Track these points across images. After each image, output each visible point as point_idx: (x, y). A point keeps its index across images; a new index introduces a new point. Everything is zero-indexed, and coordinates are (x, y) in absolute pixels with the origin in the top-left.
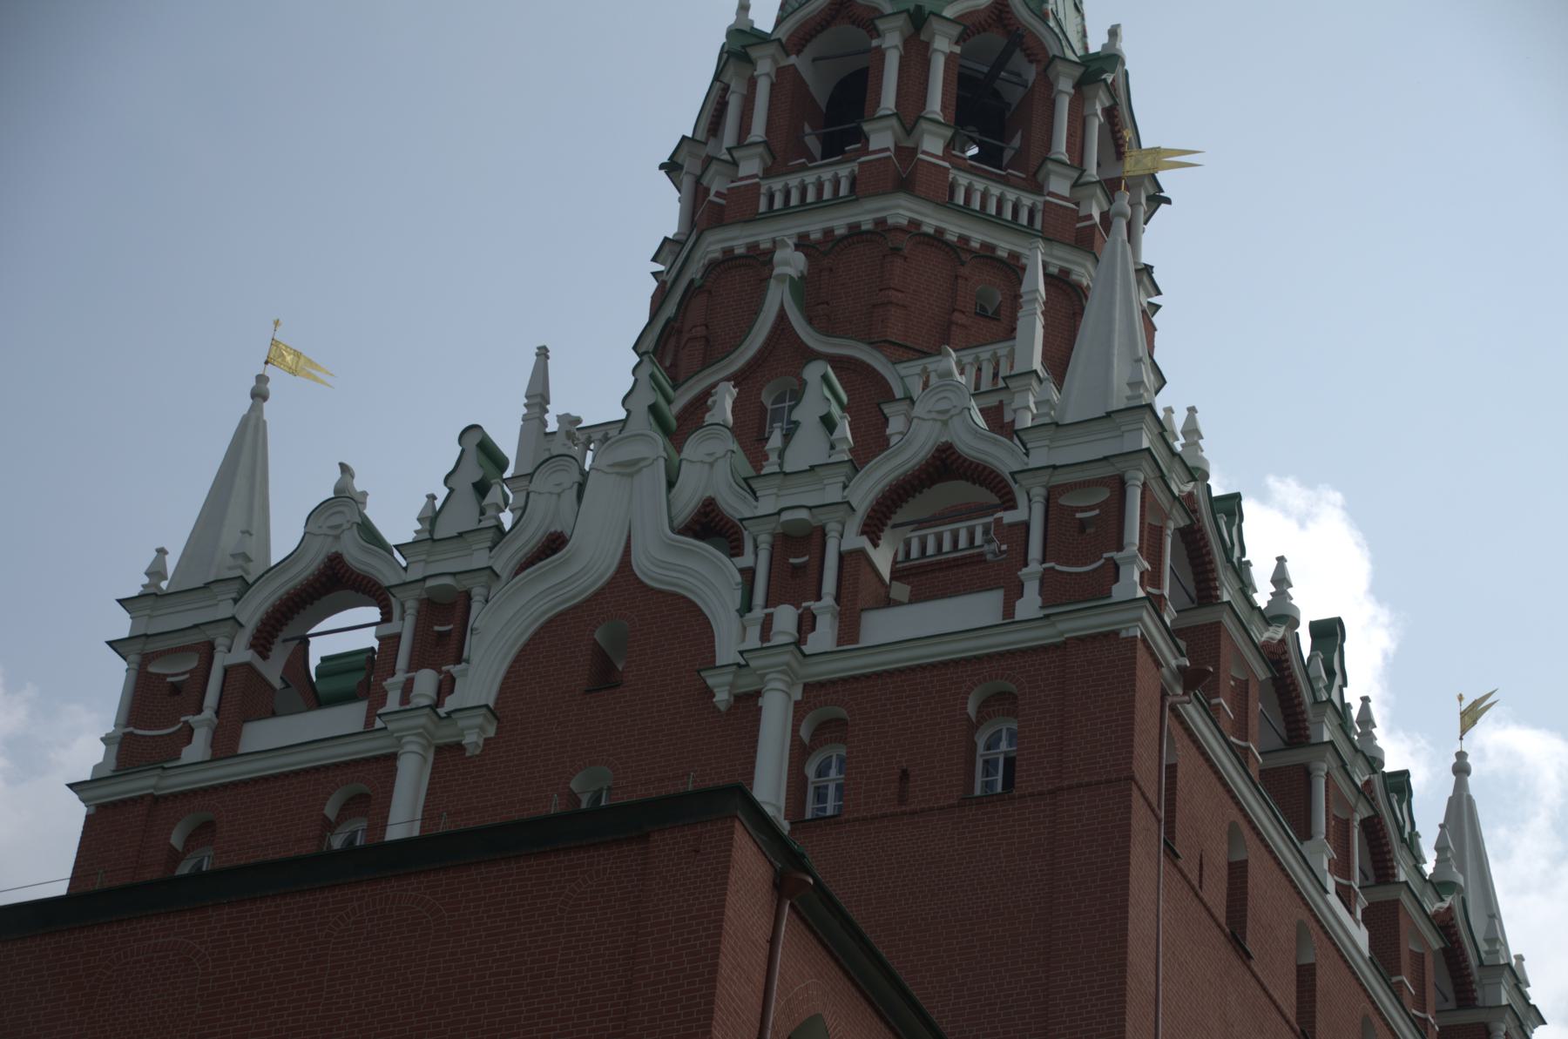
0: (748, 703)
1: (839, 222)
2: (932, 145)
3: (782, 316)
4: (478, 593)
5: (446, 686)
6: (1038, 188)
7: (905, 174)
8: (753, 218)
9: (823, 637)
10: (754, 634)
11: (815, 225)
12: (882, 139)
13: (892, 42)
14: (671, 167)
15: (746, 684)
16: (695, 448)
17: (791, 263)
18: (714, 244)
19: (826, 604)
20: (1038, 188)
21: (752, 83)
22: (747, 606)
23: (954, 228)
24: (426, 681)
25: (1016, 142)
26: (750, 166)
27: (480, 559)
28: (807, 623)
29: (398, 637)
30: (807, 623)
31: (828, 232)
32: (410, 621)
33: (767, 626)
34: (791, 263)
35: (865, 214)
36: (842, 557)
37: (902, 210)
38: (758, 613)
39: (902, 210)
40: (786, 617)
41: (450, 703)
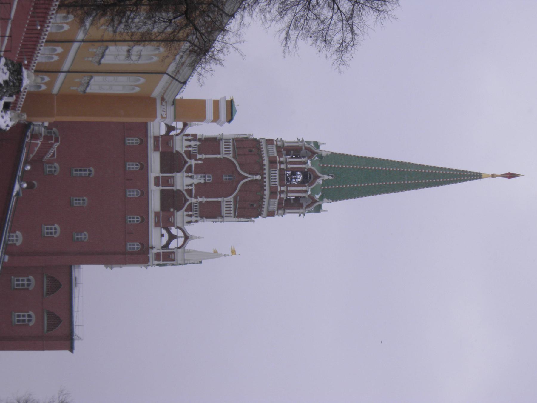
1: (267, 184)
2: (283, 196)
3: (246, 177)
6: (279, 208)
8: (270, 168)
11: (266, 180)
12: (283, 188)
17: (258, 177)
18: (266, 162)
20: (279, 208)
23: (266, 200)
26: (283, 166)
31: (265, 182)
34: (258, 177)
35: (267, 188)
37: (267, 193)
39: (267, 193)
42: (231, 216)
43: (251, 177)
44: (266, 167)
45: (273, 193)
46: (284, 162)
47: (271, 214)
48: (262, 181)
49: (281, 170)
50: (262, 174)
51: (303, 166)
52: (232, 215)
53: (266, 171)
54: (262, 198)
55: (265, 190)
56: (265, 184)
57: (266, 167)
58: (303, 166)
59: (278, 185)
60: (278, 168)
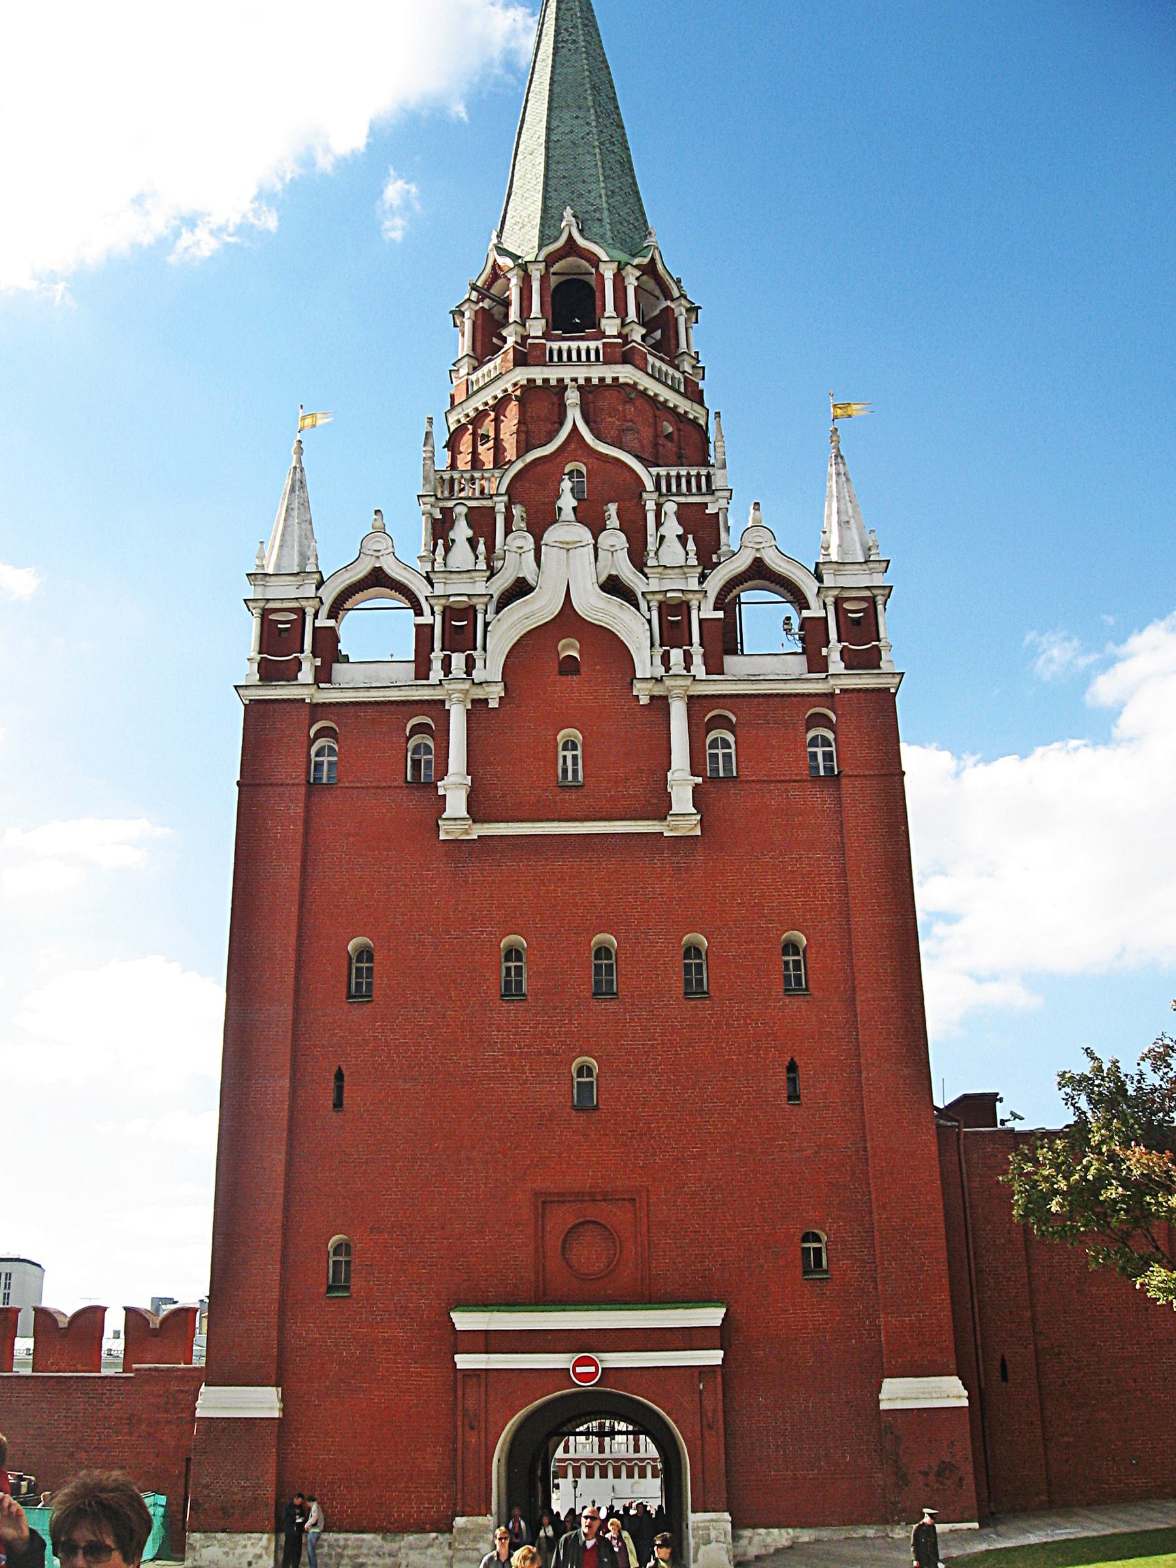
0: (661, 704)
1: (596, 373)
4: (480, 608)
5: (470, 664)
7: (623, 354)
9: (699, 669)
10: (658, 660)
11: (581, 373)
13: (608, 272)
14: (458, 313)
15: (658, 690)
16: (605, 539)
17: (572, 397)
18: (521, 375)
19: (697, 651)
21: (526, 279)
22: (652, 645)
24: (458, 660)
25: (658, 334)
27: (480, 588)
28: (688, 659)
29: (432, 626)
30: (688, 659)
32: (439, 618)
33: (666, 659)
34: (572, 397)
35: (608, 373)
36: (701, 621)
37: (626, 373)
38: (659, 651)
39: (626, 373)
40: (676, 655)
41: (477, 675)
42: (708, 477)
43: (574, 415)
44: (538, 374)
45: (627, 358)
46: (520, 329)
47: (697, 397)
48: (586, 389)
49: (546, 336)
50: (561, 386)
51: (536, 274)
52: (704, 472)
53: (553, 374)
54: (644, 393)
55: (615, 379)
56: (595, 381)
57: (538, 374)
58: (536, 274)
59: (599, 344)
60: (543, 341)
